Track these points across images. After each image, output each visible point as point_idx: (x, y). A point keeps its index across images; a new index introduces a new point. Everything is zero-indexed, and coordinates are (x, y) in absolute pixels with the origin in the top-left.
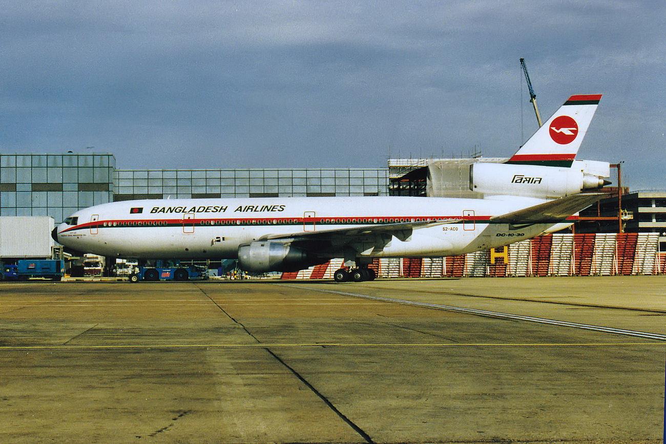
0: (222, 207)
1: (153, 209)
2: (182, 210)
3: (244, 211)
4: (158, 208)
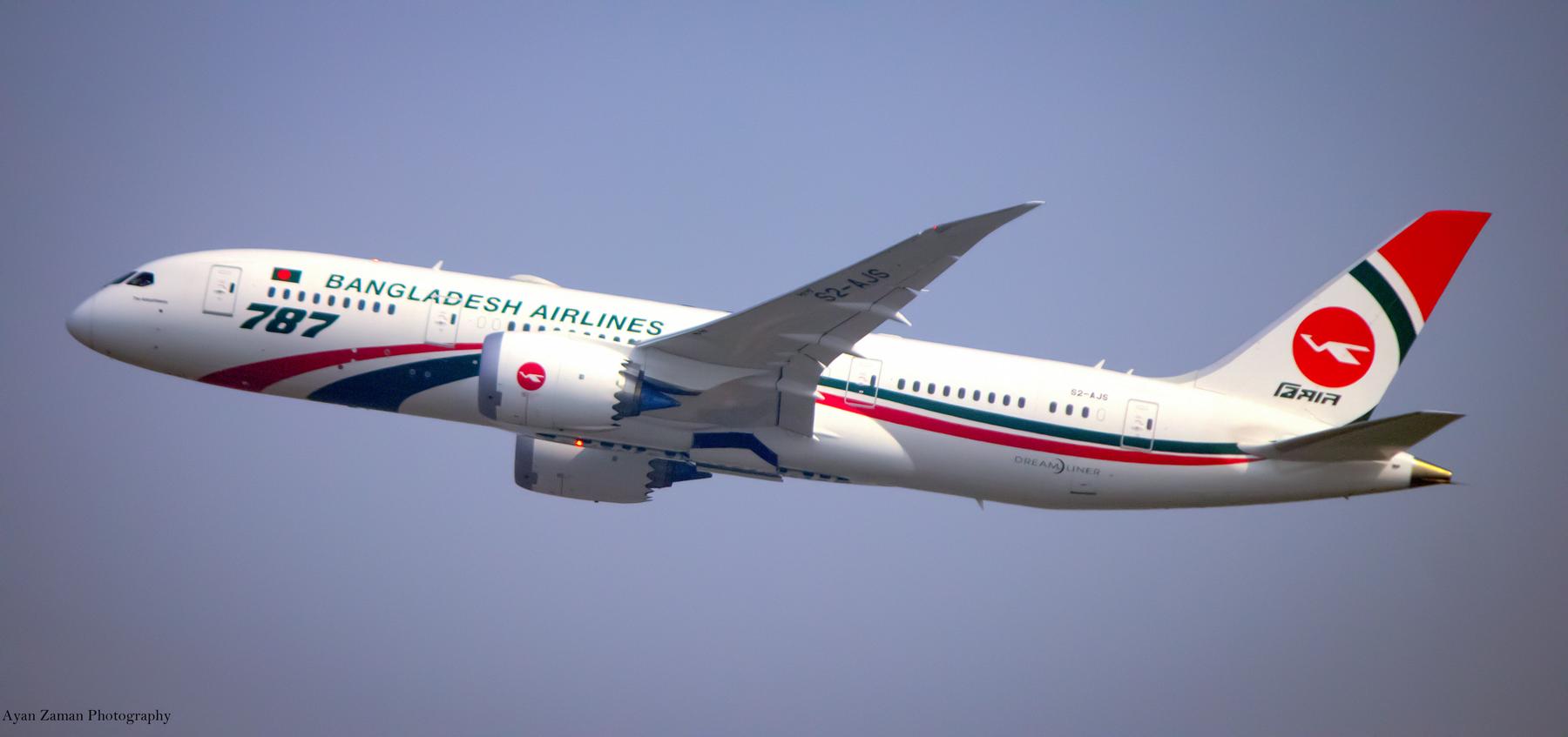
1: (331, 280)
2: (407, 292)
3: (553, 318)
4: (342, 278)
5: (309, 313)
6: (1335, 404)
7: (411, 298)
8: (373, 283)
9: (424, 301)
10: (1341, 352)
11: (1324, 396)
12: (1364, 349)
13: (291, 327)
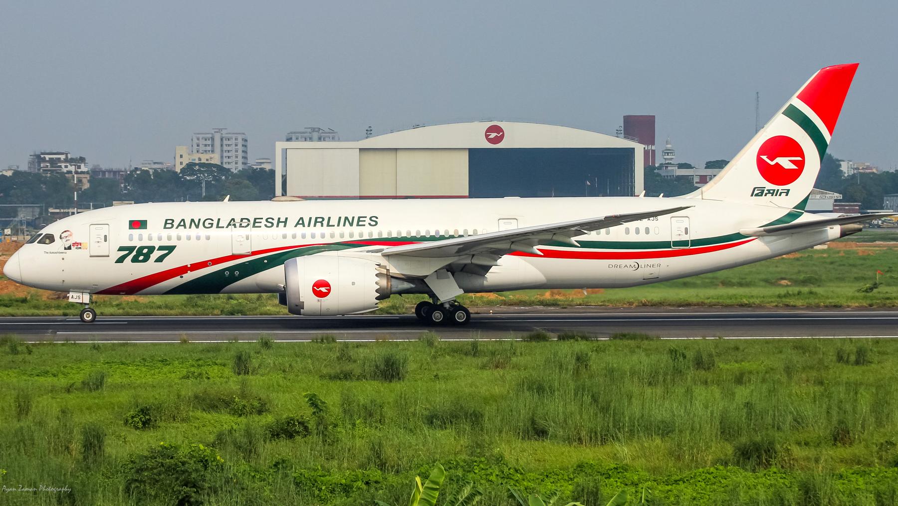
0: (279, 219)
1: (166, 223)
3: (309, 225)
4: (173, 221)
5: (156, 249)
6: (787, 195)
7: (218, 227)
8: (192, 220)
9: (227, 227)
10: (785, 162)
11: (780, 191)
12: (799, 159)
13: (146, 259)
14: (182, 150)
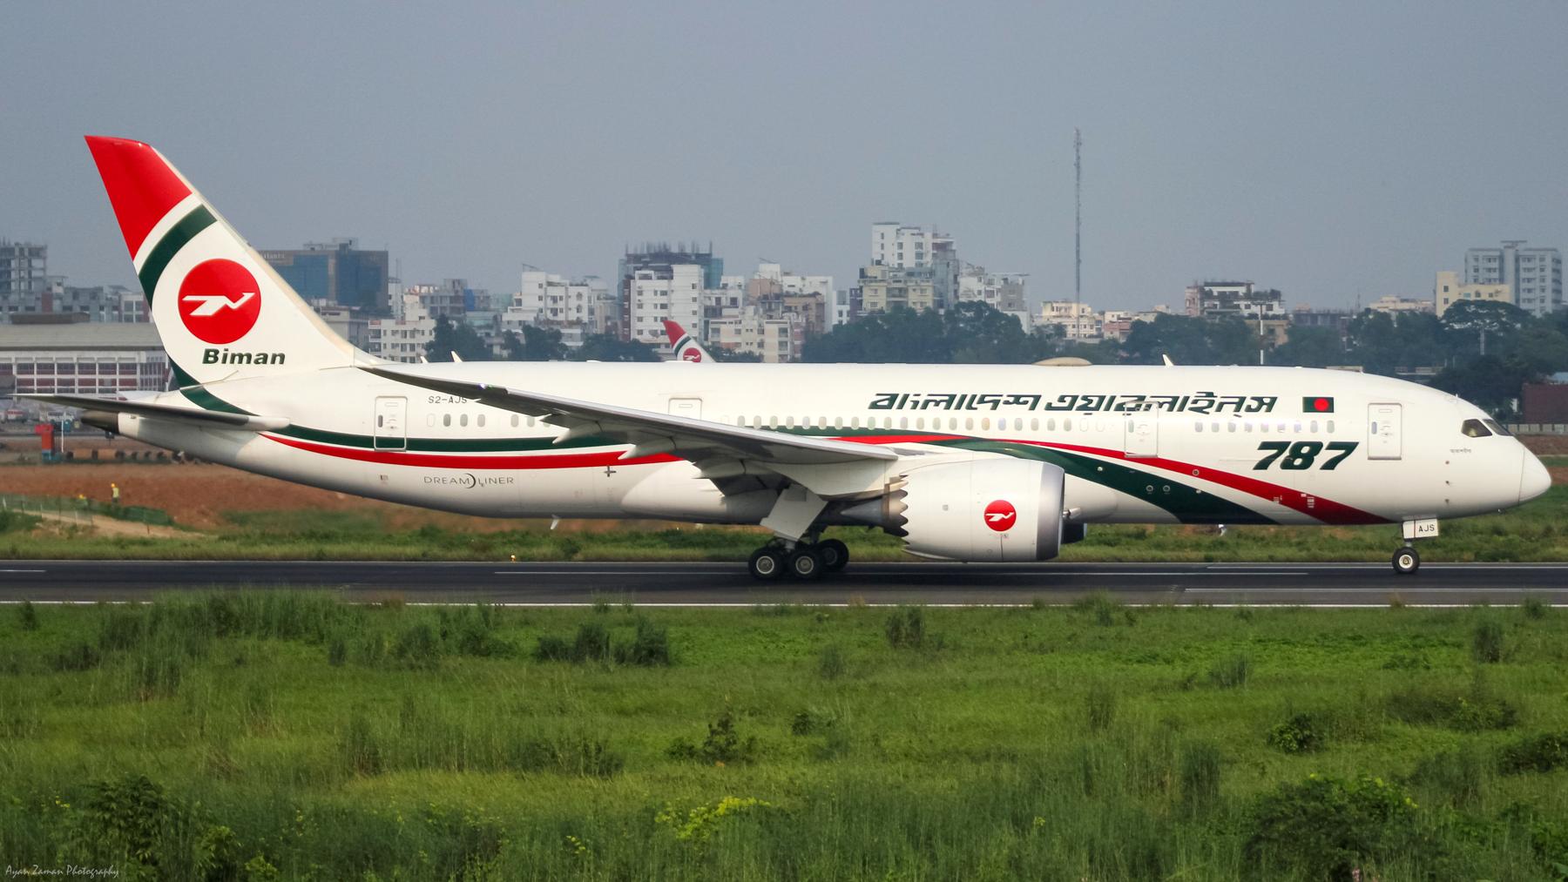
14: (1448, 278)
